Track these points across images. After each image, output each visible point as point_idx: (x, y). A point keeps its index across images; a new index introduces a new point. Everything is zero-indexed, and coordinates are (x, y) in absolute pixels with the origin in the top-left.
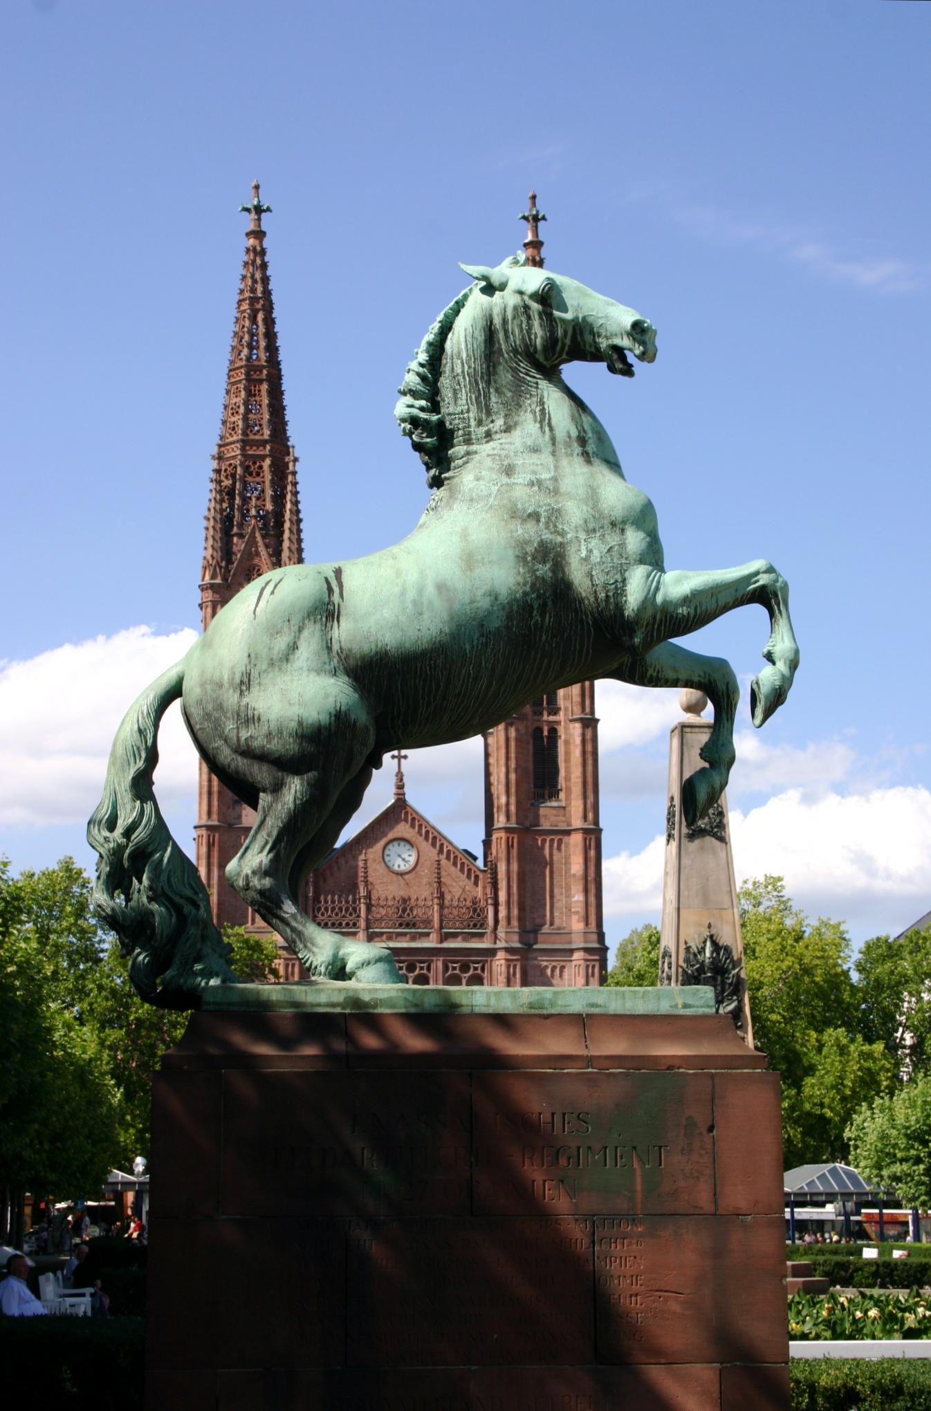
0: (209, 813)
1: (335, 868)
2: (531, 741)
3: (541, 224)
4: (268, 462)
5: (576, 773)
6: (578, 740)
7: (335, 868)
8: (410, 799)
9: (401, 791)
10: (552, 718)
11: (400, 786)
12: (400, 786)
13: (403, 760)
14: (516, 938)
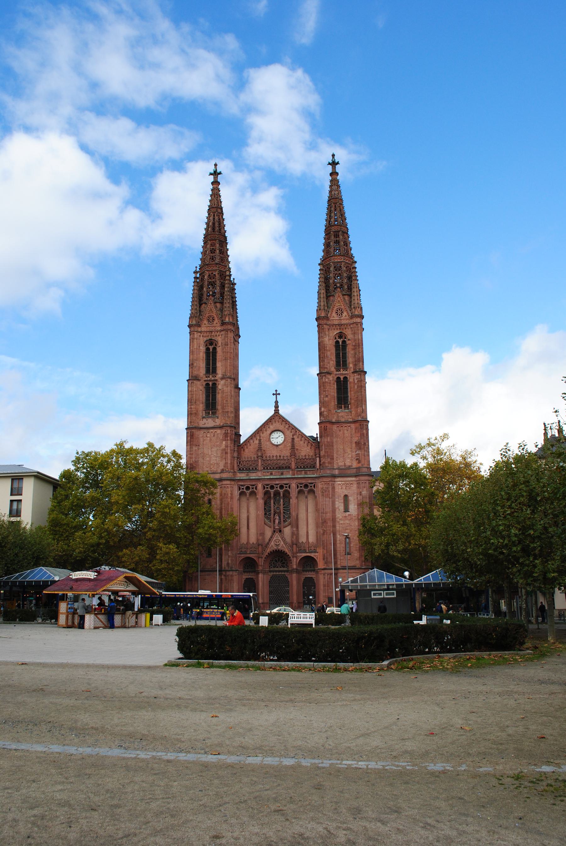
1: (249, 445)
2: (335, 383)
3: (337, 166)
7: (249, 445)
8: (281, 412)
9: (277, 409)
10: (344, 372)
11: (277, 407)
12: (277, 407)
13: (278, 396)
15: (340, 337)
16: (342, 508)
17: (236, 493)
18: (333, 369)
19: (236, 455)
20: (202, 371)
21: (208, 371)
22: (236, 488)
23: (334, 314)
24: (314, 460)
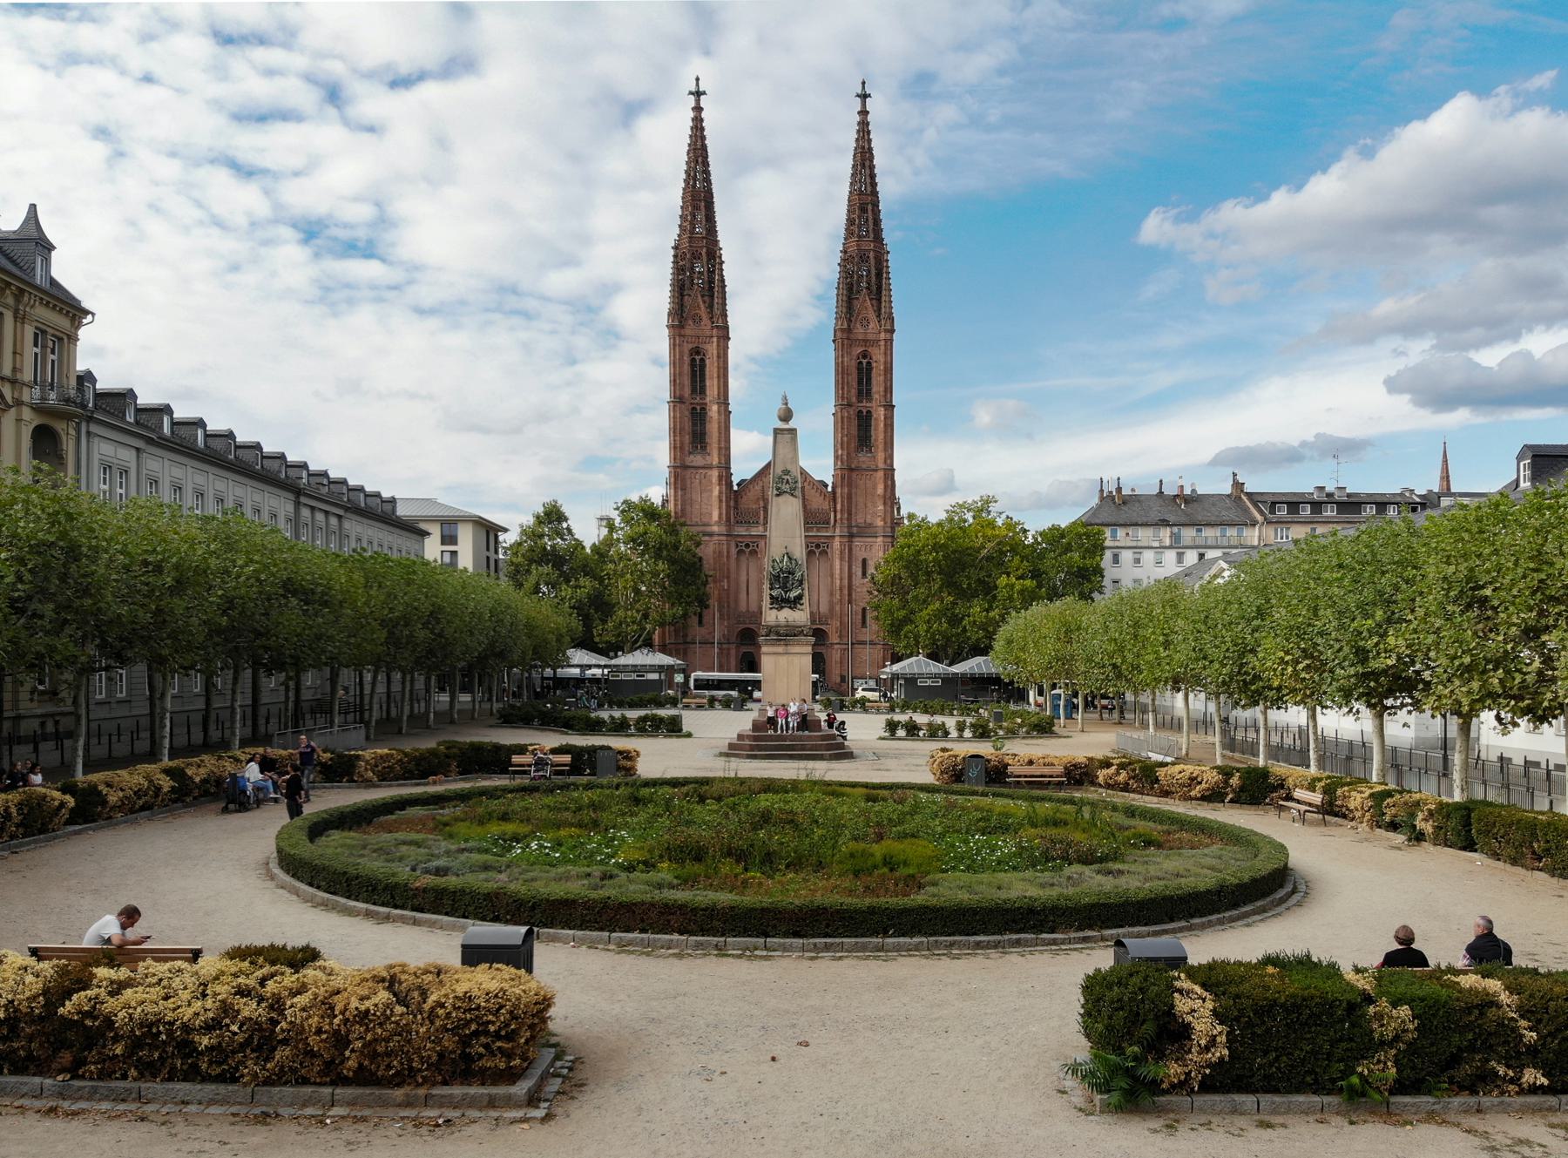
0: (675, 459)
4: (704, 250)
5: (881, 437)
6: (882, 418)
10: (868, 405)
14: (846, 530)
15: (865, 357)
16: (860, 573)
17: (734, 551)
18: (854, 400)
19: (732, 503)
20: (687, 392)
21: (694, 391)
22: (733, 544)
23: (858, 325)
24: (828, 514)
